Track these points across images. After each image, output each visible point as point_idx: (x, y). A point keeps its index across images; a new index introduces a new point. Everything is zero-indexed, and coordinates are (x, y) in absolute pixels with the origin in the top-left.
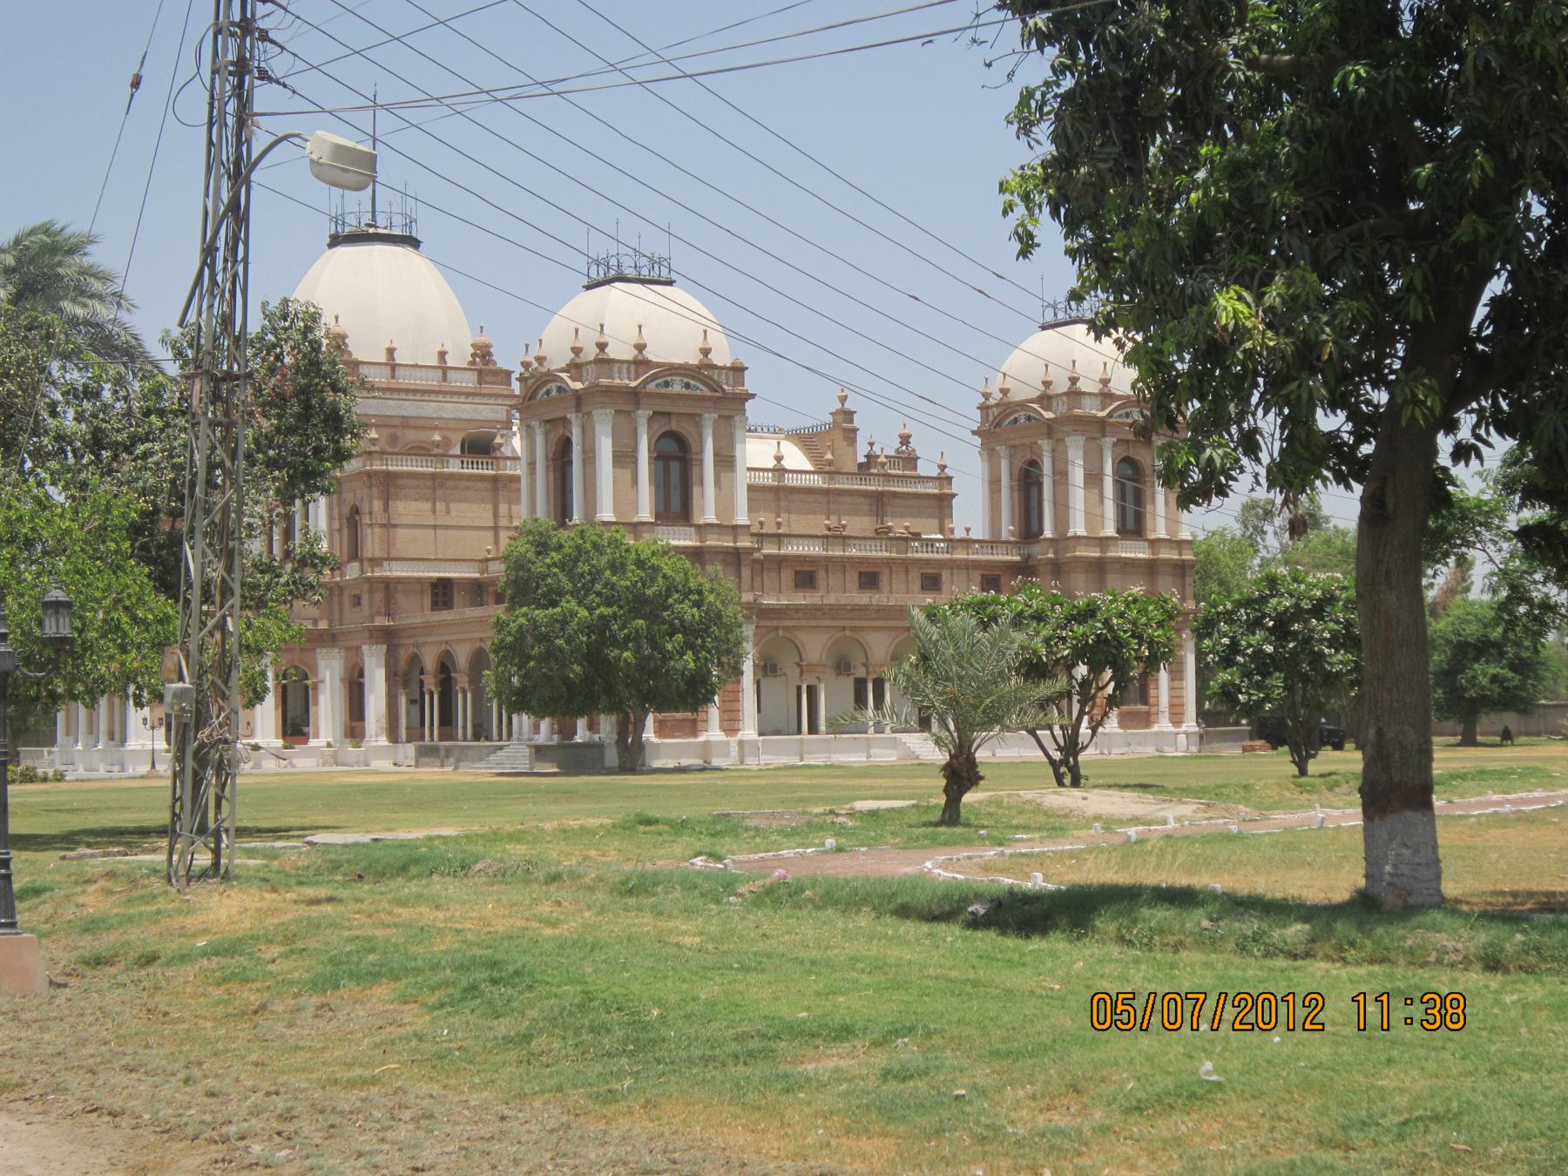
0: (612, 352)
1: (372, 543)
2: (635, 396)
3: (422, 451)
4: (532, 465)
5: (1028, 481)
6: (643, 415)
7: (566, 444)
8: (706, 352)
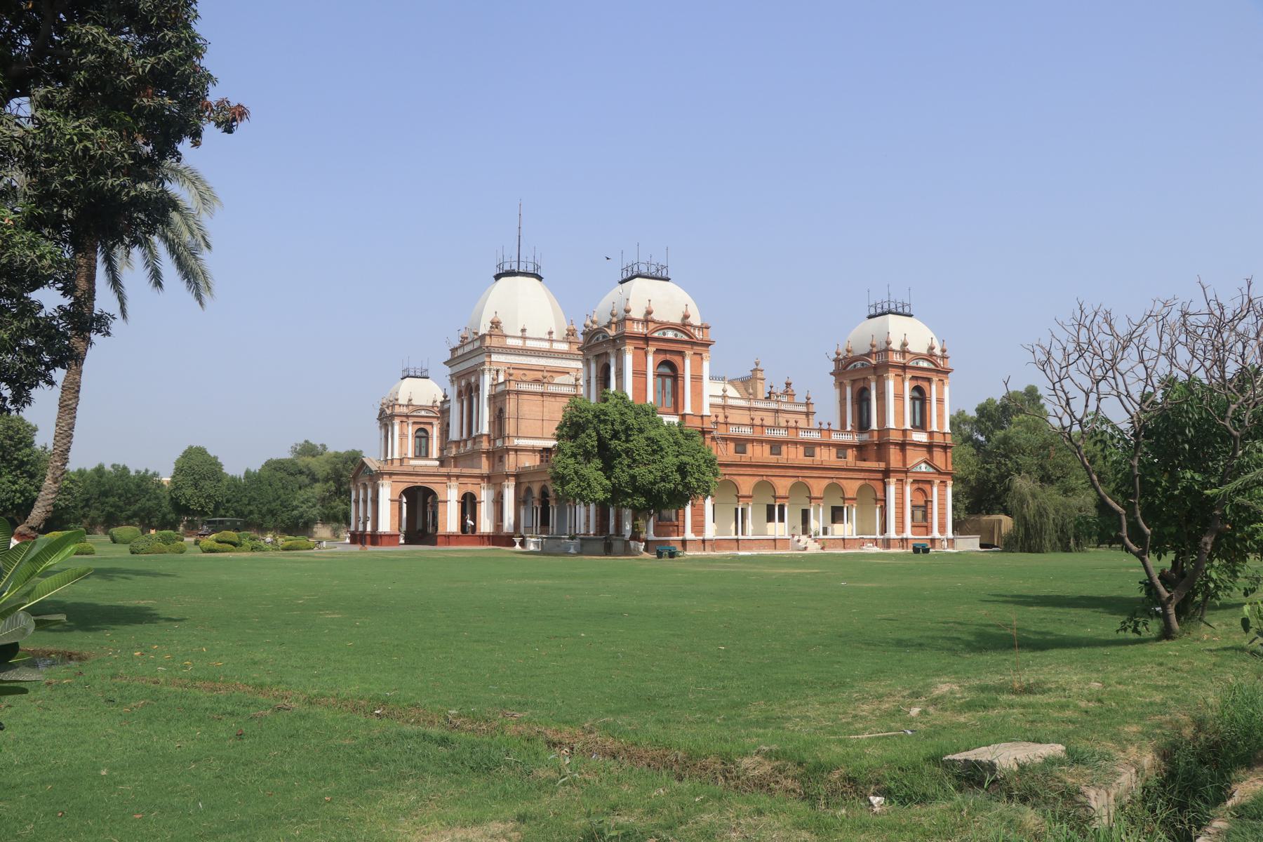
1: (510, 427)
2: (646, 339)
3: (537, 381)
4: (588, 382)
5: (861, 399)
6: (651, 349)
7: (606, 369)
8: (686, 317)
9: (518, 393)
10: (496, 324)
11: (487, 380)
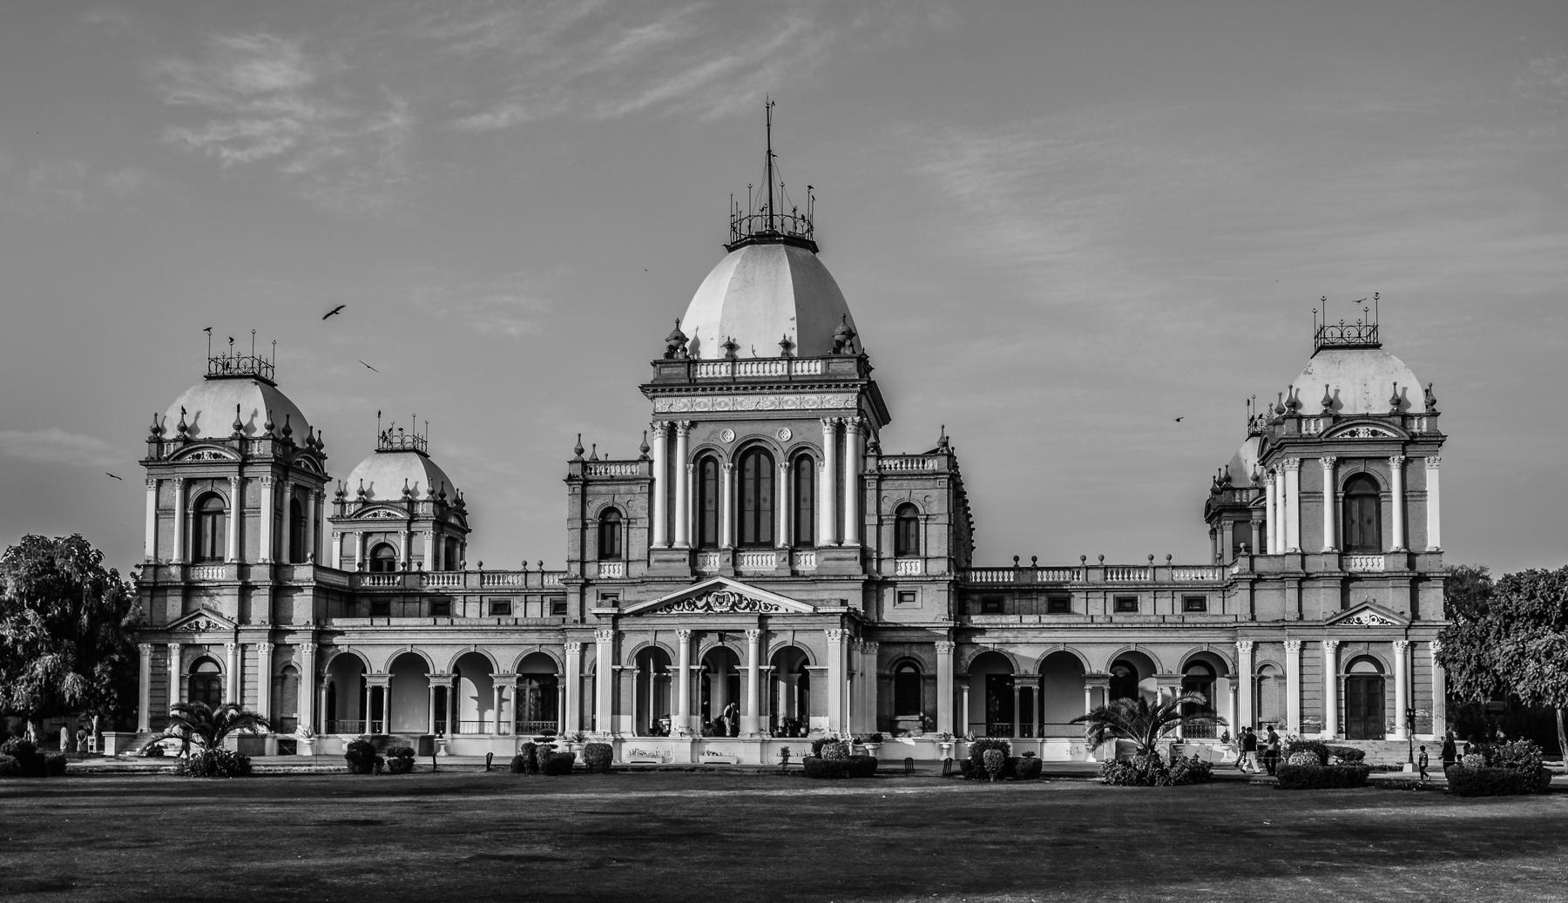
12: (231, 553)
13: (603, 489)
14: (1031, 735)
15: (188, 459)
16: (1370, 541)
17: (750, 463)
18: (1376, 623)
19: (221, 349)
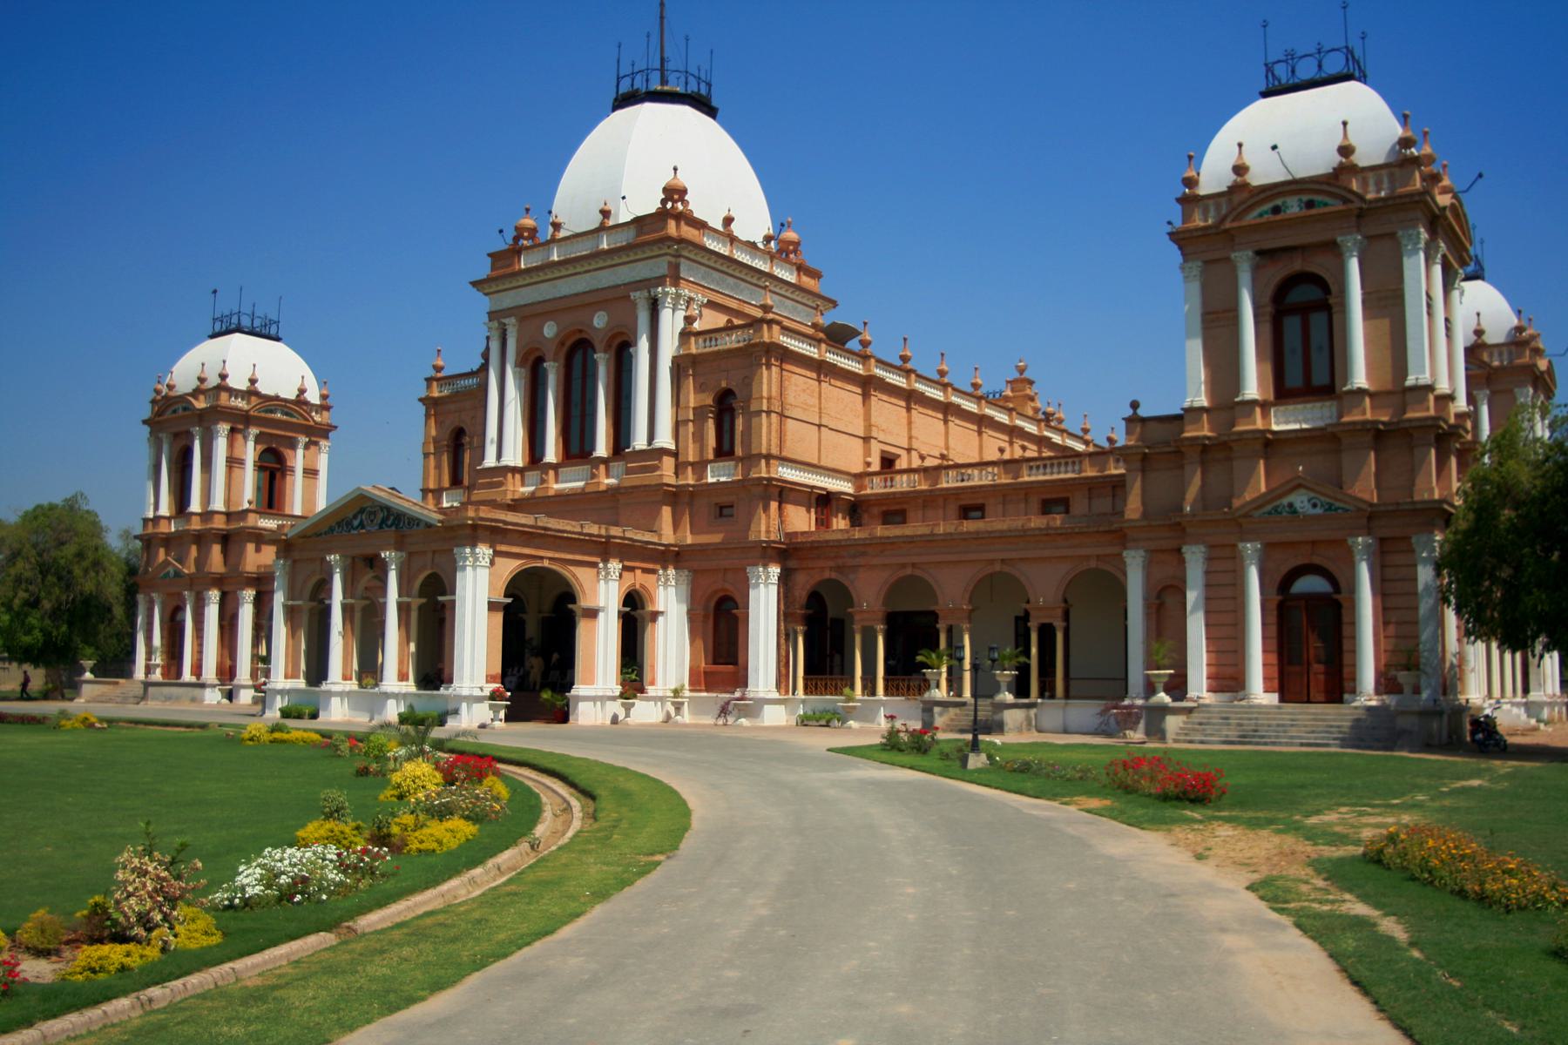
0: (1362, 159)
1: (766, 435)
9: (786, 356)
10: (674, 193)
11: (671, 322)
12: (195, 506)
13: (452, 407)
14: (873, 693)
15: (168, 415)
16: (1320, 378)
17: (578, 358)
18: (1319, 511)
19: (224, 308)
